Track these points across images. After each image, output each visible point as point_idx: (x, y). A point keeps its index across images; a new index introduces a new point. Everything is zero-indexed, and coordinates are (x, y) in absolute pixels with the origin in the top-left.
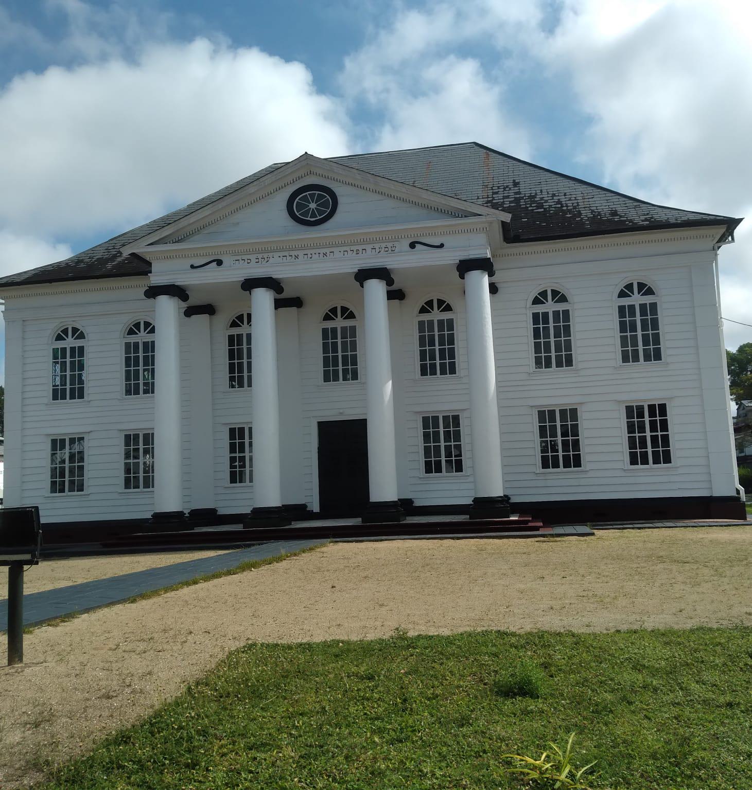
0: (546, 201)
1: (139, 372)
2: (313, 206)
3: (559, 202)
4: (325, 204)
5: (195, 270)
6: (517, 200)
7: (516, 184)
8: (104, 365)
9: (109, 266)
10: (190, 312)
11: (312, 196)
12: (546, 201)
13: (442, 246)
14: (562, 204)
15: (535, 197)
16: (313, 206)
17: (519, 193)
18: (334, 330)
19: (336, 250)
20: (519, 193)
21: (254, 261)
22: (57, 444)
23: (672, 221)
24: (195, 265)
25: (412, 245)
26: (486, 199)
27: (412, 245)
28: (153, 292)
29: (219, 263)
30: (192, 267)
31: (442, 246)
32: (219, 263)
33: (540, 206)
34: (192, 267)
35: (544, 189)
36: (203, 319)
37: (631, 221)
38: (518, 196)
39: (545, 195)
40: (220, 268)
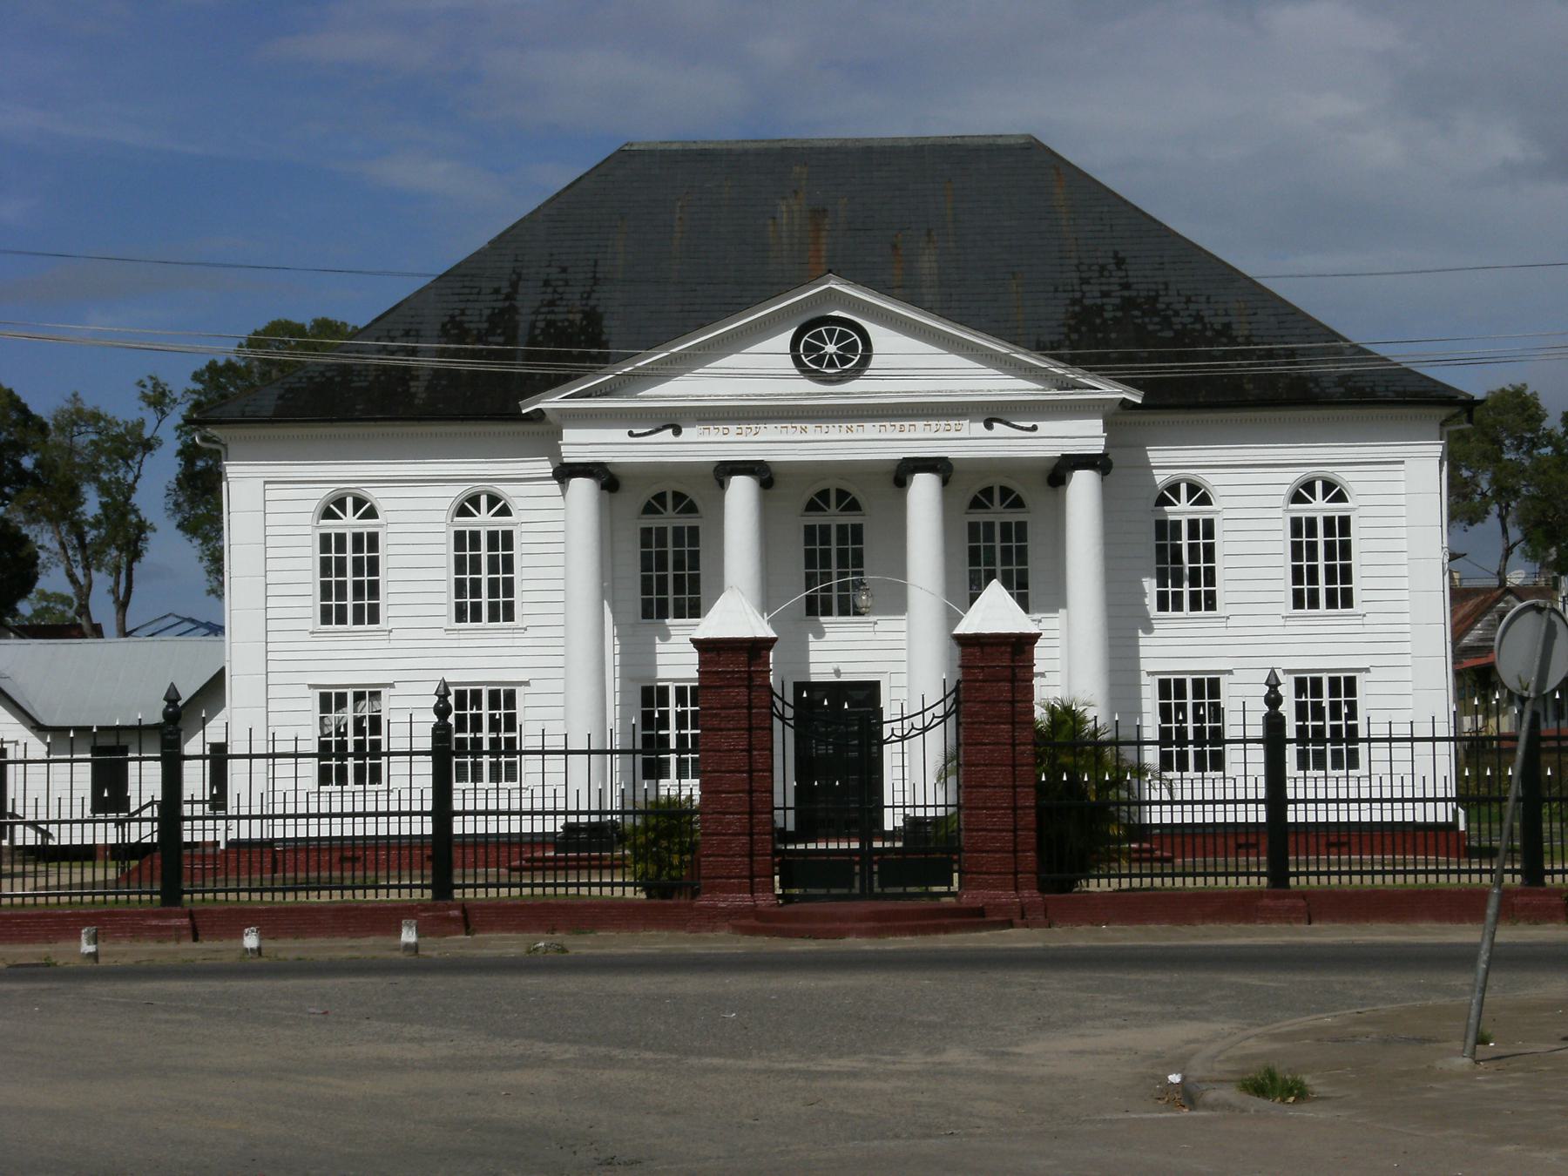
0: (1177, 314)
1: (484, 581)
2: (831, 348)
3: (1198, 318)
6: (1128, 304)
7: (1120, 262)
8: (416, 565)
12: (1177, 314)
13: (1034, 428)
14: (1204, 325)
15: (1155, 299)
16: (831, 348)
17: (1126, 286)
18: (825, 530)
22: (330, 701)
24: (636, 431)
26: (1071, 295)
28: (565, 473)
31: (1034, 428)
38: (1126, 293)
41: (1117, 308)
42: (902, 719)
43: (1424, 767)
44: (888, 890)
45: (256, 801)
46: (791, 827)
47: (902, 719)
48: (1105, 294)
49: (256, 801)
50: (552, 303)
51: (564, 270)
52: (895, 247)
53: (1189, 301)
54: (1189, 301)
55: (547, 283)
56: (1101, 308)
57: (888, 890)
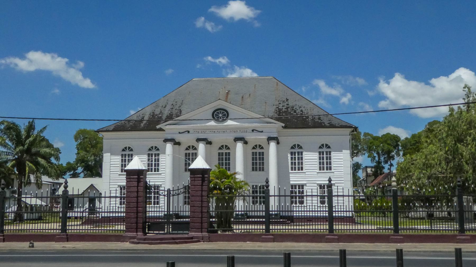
2: (220, 115)
3: (302, 111)
4: (225, 115)
5: (181, 135)
6: (287, 108)
7: (287, 100)
9: (142, 125)
10: (174, 144)
11: (220, 112)
13: (262, 132)
17: (288, 105)
19: (228, 130)
20: (288, 105)
21: (200, 132)
23: (337, 125)
25: (253, 131)
27: (253, 131)
28: (166, 141)
29: (189, 132)
30: (179, 133)
31: (262, 132)
32: (189, 132)
33: (295, 112)
34: (179, 133)
35: (297, 104)
36: (177, 146)
37: (324, 123)
39: (297, 107)
40: (189, 135)
41: (285, 109)
42: (178, 190)
43: (346, 203)
44: (173, 232)
45: (106, 208)
46: (214, 215)
47: (178, 190)
48: (283, 106)
49: (106, 208)
50: (172, 108)
51: (176, 102)
52: (242, 97)
53: (300, 107)
54: (300, 107)
55: (172, 105)
56: (282, 109)
57: (173, 232)
